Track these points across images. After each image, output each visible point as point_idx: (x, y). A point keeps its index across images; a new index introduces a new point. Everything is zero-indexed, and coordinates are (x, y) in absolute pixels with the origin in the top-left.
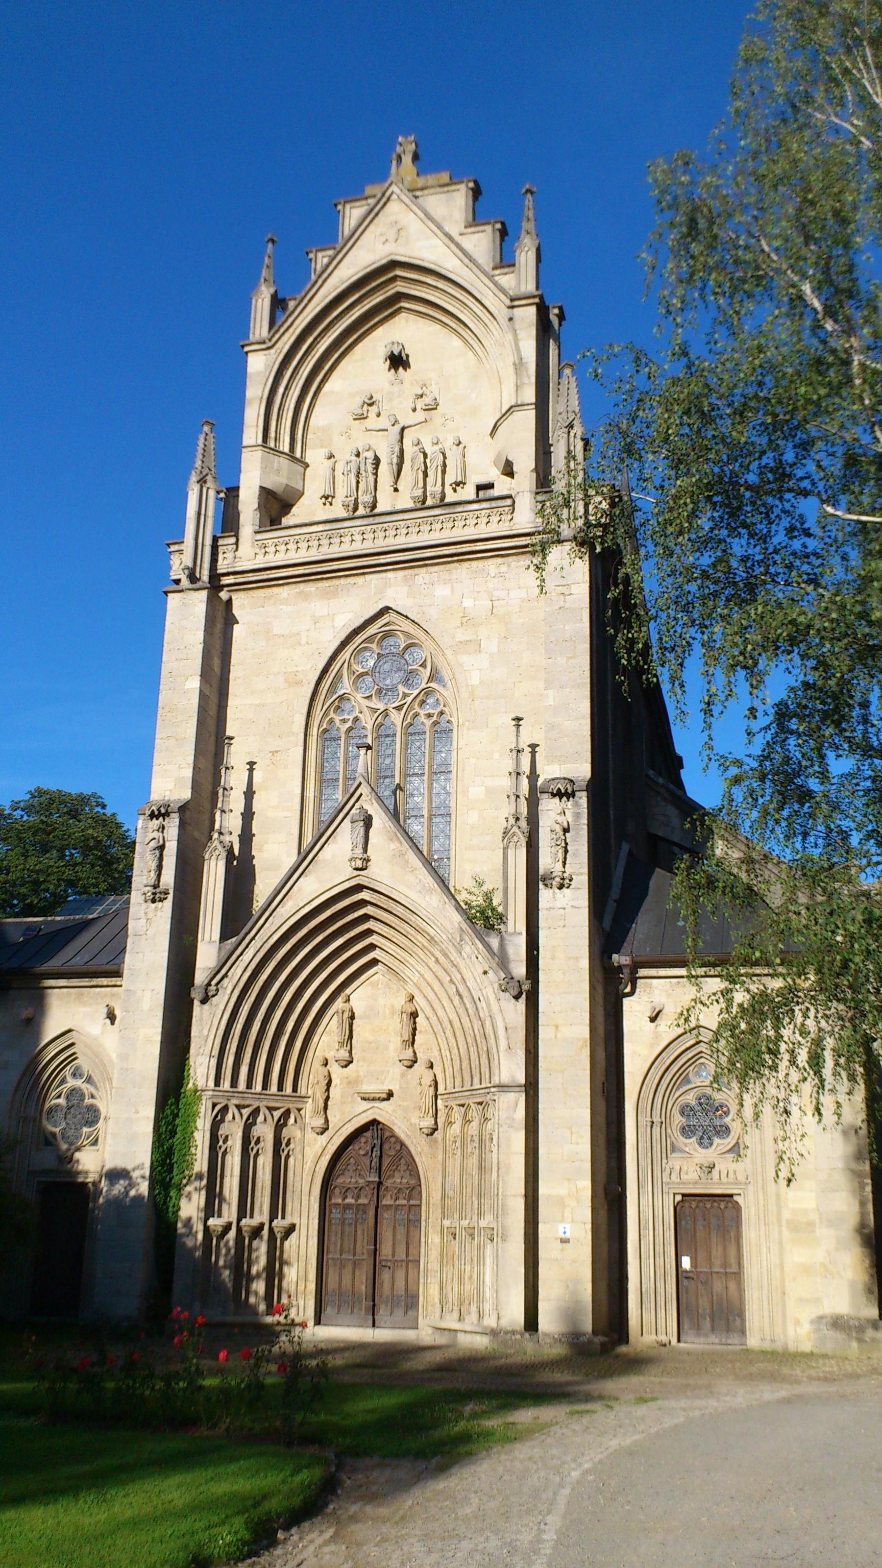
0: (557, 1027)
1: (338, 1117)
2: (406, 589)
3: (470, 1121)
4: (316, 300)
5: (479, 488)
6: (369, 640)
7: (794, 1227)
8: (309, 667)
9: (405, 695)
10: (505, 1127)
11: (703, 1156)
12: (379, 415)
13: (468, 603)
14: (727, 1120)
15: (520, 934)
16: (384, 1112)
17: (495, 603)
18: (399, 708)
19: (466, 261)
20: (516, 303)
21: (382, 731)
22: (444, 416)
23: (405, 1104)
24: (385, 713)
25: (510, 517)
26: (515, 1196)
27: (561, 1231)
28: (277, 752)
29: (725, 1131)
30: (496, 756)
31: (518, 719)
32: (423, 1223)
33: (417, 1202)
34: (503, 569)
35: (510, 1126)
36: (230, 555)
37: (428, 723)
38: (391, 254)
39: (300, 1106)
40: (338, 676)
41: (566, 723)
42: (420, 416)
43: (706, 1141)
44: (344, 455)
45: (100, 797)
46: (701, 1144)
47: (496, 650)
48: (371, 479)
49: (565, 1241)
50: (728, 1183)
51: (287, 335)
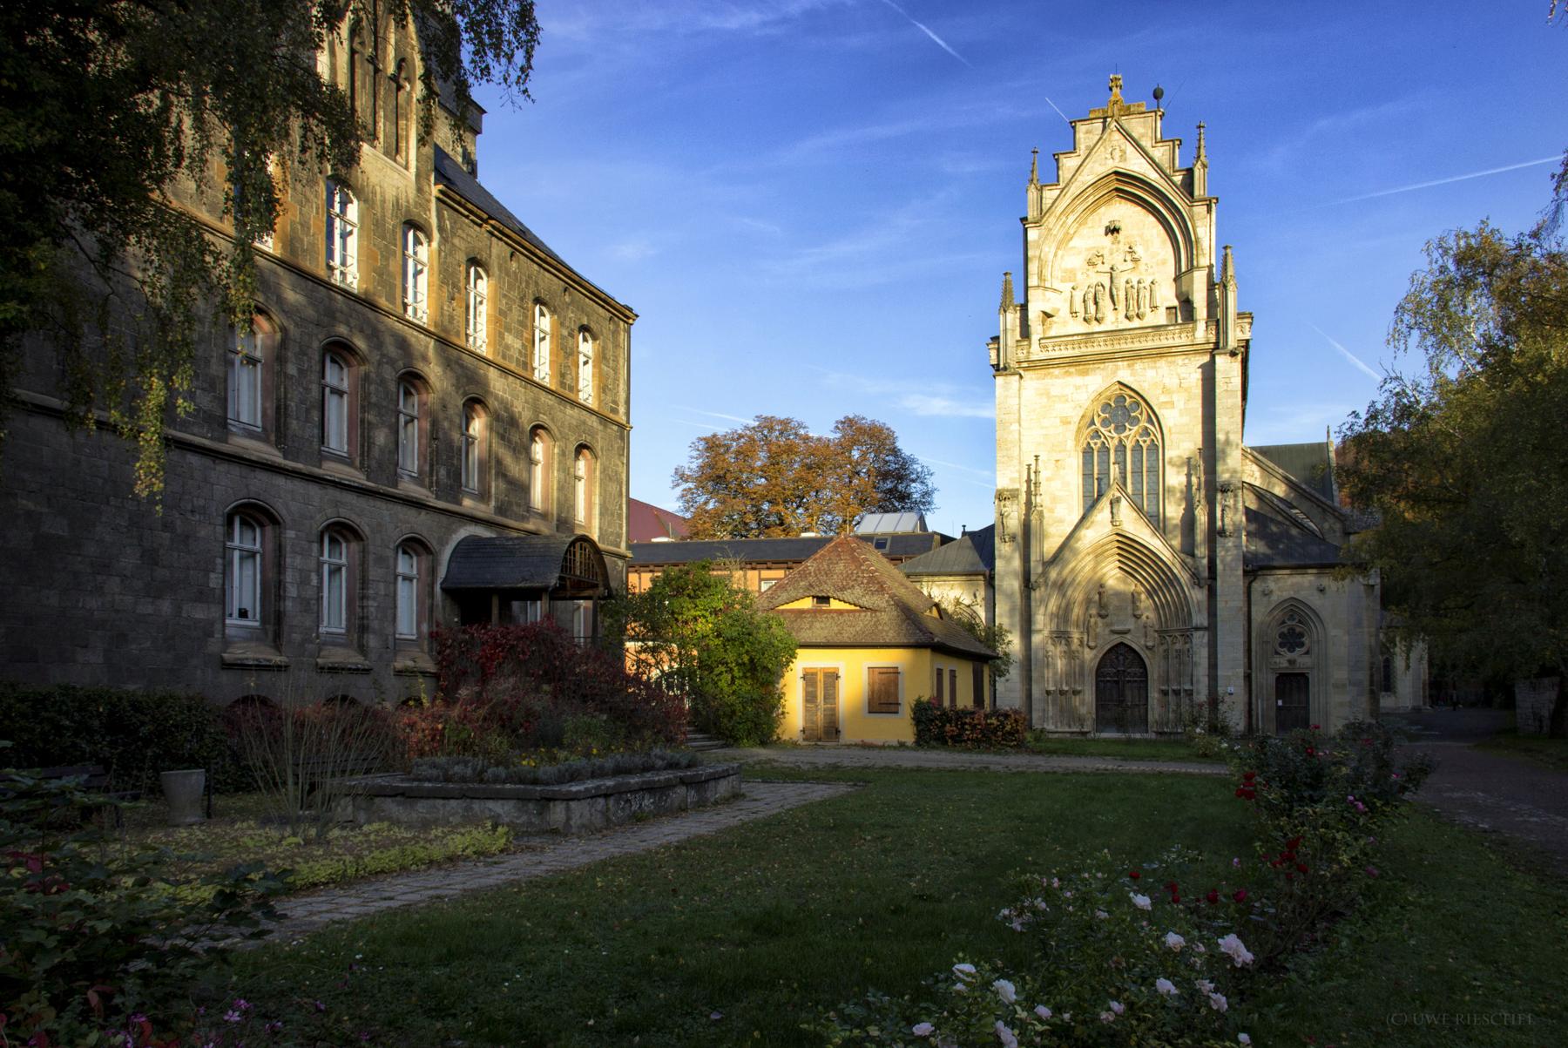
7: (1336, 686)
11: (1289, 655)
13: (1167, 381)
16: (1128, 639)
29: (1302, 645)
45: (800, 425)
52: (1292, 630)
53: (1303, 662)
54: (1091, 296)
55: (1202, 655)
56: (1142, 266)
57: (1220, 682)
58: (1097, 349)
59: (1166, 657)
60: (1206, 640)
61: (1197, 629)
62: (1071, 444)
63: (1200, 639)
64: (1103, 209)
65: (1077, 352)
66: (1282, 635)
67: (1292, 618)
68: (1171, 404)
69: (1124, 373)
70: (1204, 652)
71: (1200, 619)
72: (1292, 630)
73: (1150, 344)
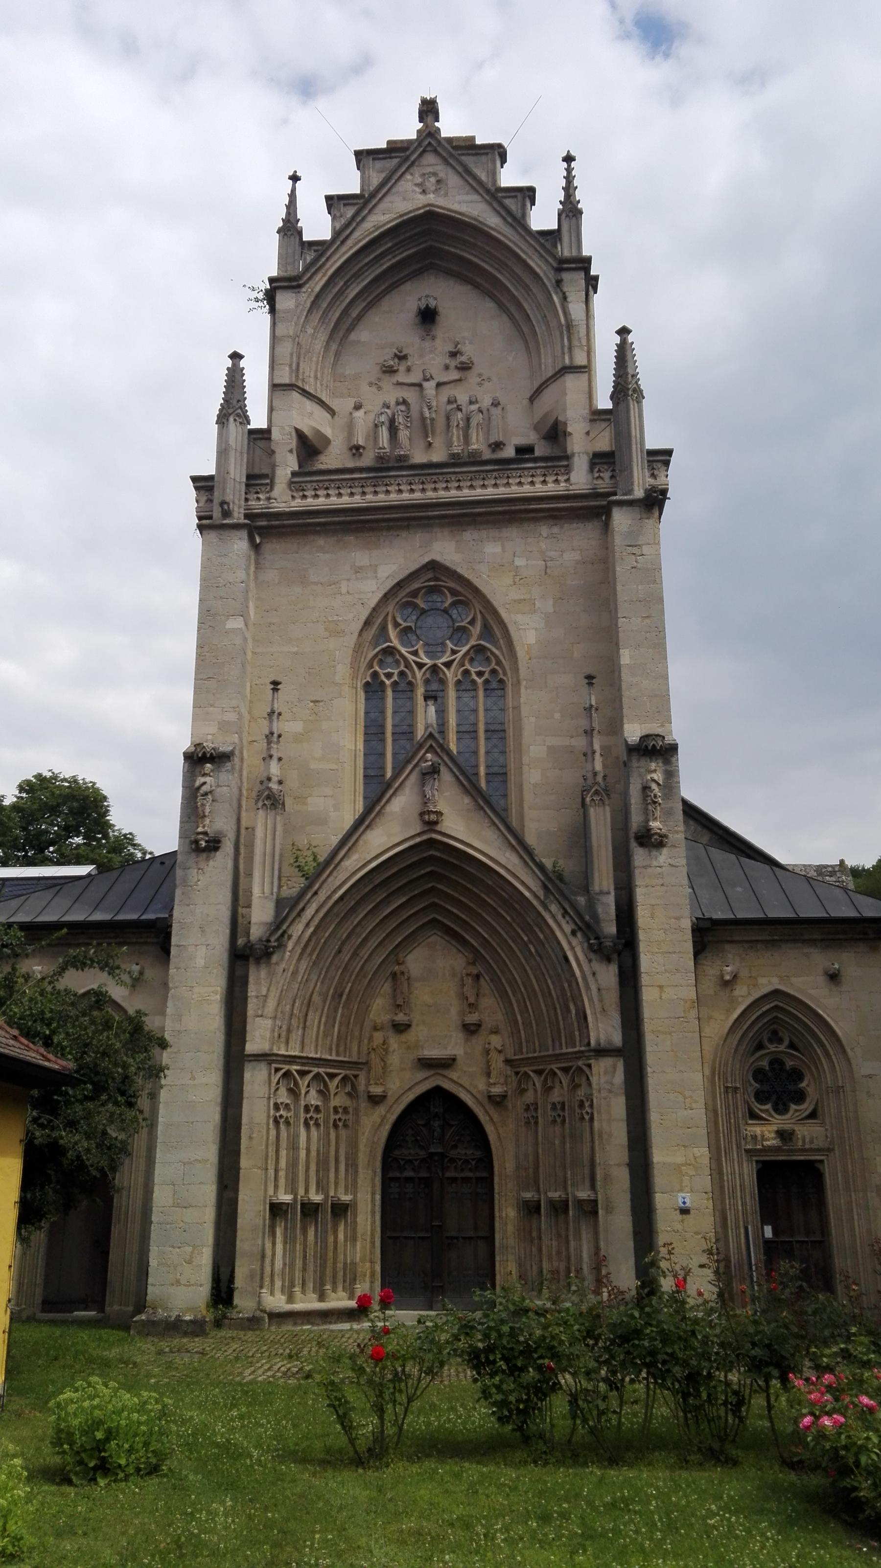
0: (661, 987)
1: (398, 1084)
2: (453, 544)
3: (551, 1088)
4: (349, 242)
5: (520, 450)
6: (415, 594)
8: (351, 616)
9: (454, 652)
10: (604, 1094)
11: (779, 1122)
12: (409, 370)
14: (803, 1085)
15: (608, 893)
17: (549, 564)
18: (448, 665)
19: (510, 220)
20: (566, 266)
22: (480, 375)
23: (471, 1070)
24: (434, 669)
25: (566, 477)
26: (619, 1165)
27: (680, 1201)
30: (557, 716)
32: (496, 1196)
33: (485, 1174)
34: (556, 530)
35: (610, 1091)
38: (429, 205)
39: (356, 1073)
40: (383, 629)
42: (454, 375)
43: (781, 1107)
46: (777, 1110)
47: (551, 610)
49: (685, 1211)
50: (811, 1150)
51: (320, 275)
52: (777, 1063)
53: (809, 1134)
54: (383, 418)
55: (612, 1113)
56: (472, 378)
57: (660, 1179)
59: (532, 1123)
60: (619, 1077)
61: (601, 1052)
62: (343, 671)
63: (607, 1076)
64: (408, 286)
66: (759, 1074)
67: (776, 1038)
69: (446, 549)
70: (618, 1107)
71: (606, 1028)
72: (777, 1063)
73: (490, 492)
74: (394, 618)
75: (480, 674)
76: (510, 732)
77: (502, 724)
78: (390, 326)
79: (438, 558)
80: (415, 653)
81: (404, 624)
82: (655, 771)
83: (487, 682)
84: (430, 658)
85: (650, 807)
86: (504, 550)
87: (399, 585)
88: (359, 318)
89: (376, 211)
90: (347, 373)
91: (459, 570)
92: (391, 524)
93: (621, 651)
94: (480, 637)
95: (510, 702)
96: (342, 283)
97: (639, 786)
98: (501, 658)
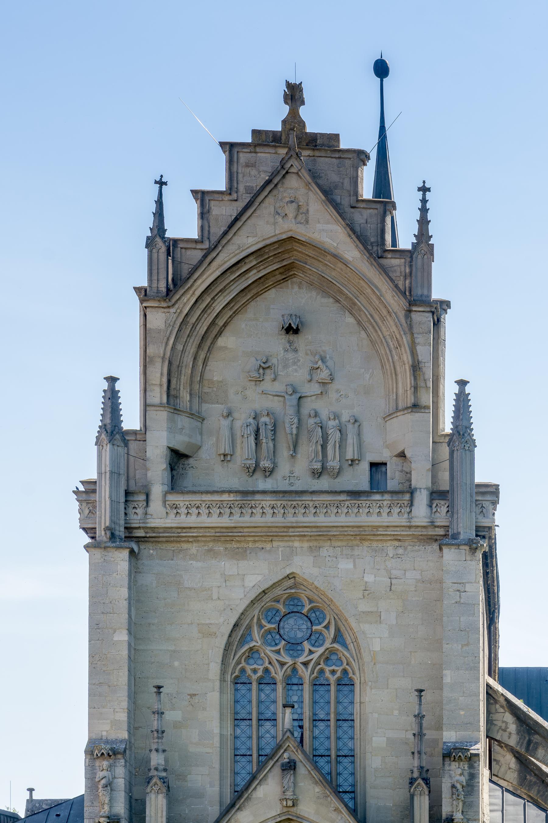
2: (311, 559)
4: (215, 264)
18: (305, 664)
21: (292, 681)
28: (195, 695)
31: (421, 691)
36: (140, 511)
37: (333, 679)
41: (460, 698)
44: (242, 418)
48: (271, 444)
58: (258, 519)
65: (225, 521)
68: (376, 617)
74: (259, 619)
75: (333, 672)
76: (357, 723)
77: (352, 714)
78: (252, 335)
79: (297, 571)
80: (278, 652)
81: (269, 626)
82: (461, 775)
83: (339, 679)
84: (291, 656)
85: (454, 802)
86: (355, 565)
87: (264, 592)
88: (225, 325)
89: (241, 233)
90: (215, 379)
91: (316, 583)
92: (257, 539)
93: (445, 672)
94: (334, 640)
95: (357, 699)
96: (209, 299)
97: (450, 785)
98: (351, 659)
